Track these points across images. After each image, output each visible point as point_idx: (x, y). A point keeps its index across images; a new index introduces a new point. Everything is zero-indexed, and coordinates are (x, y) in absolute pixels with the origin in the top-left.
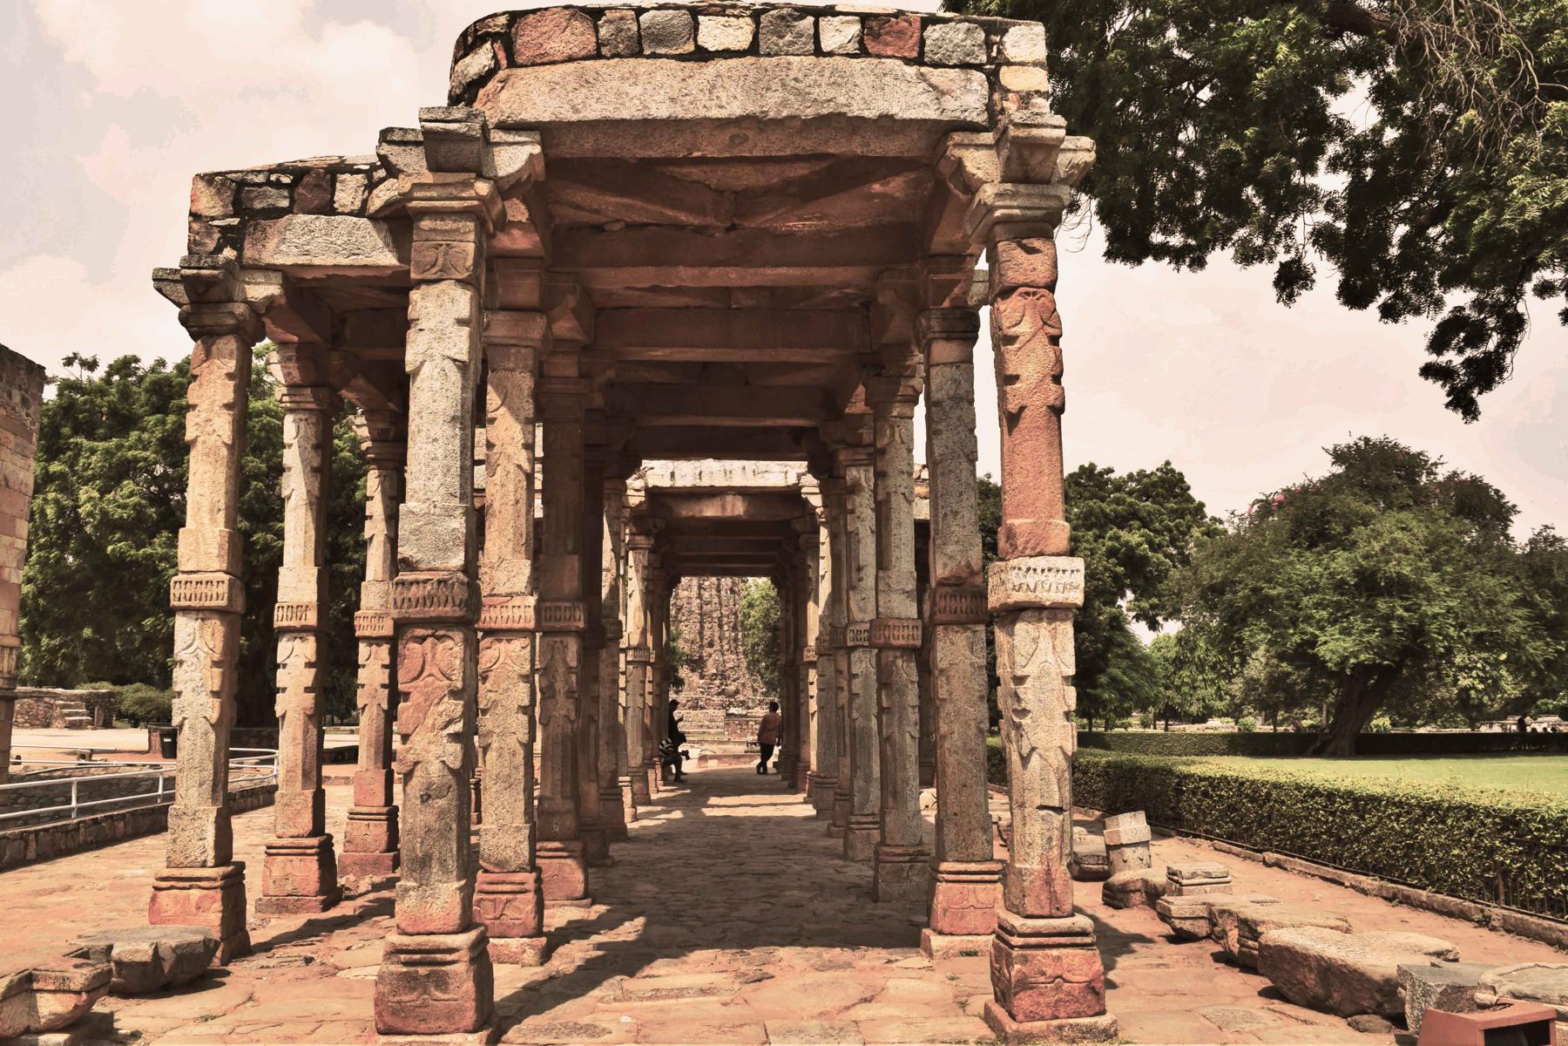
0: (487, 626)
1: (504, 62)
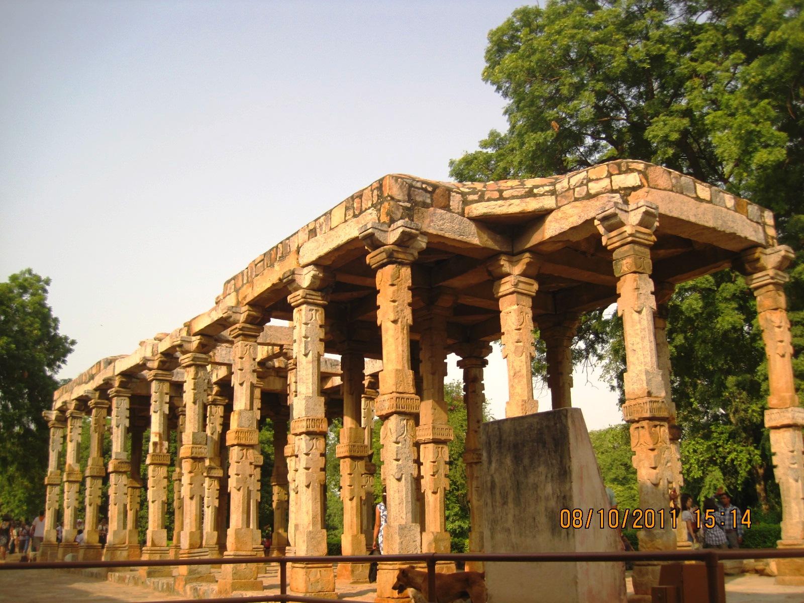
1: (646, 184)
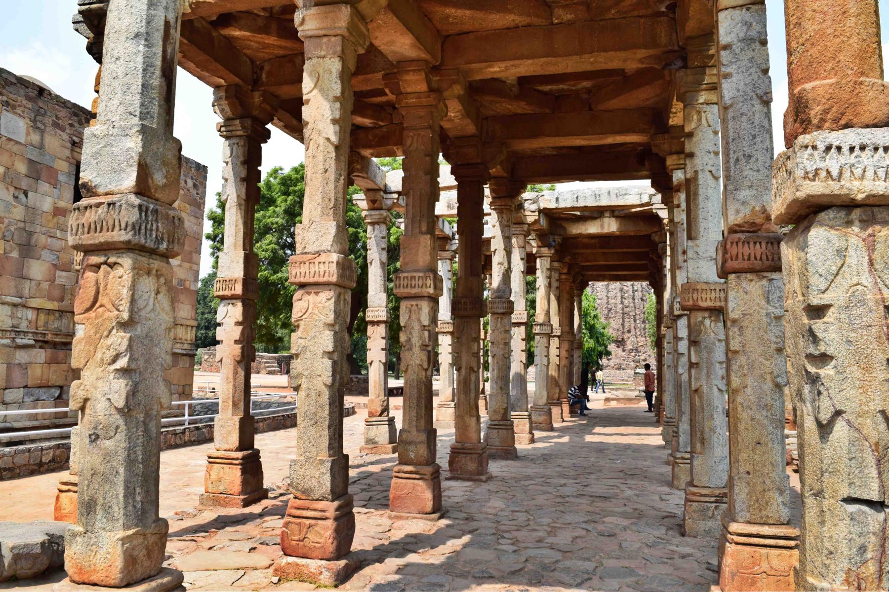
0: (298, 280)
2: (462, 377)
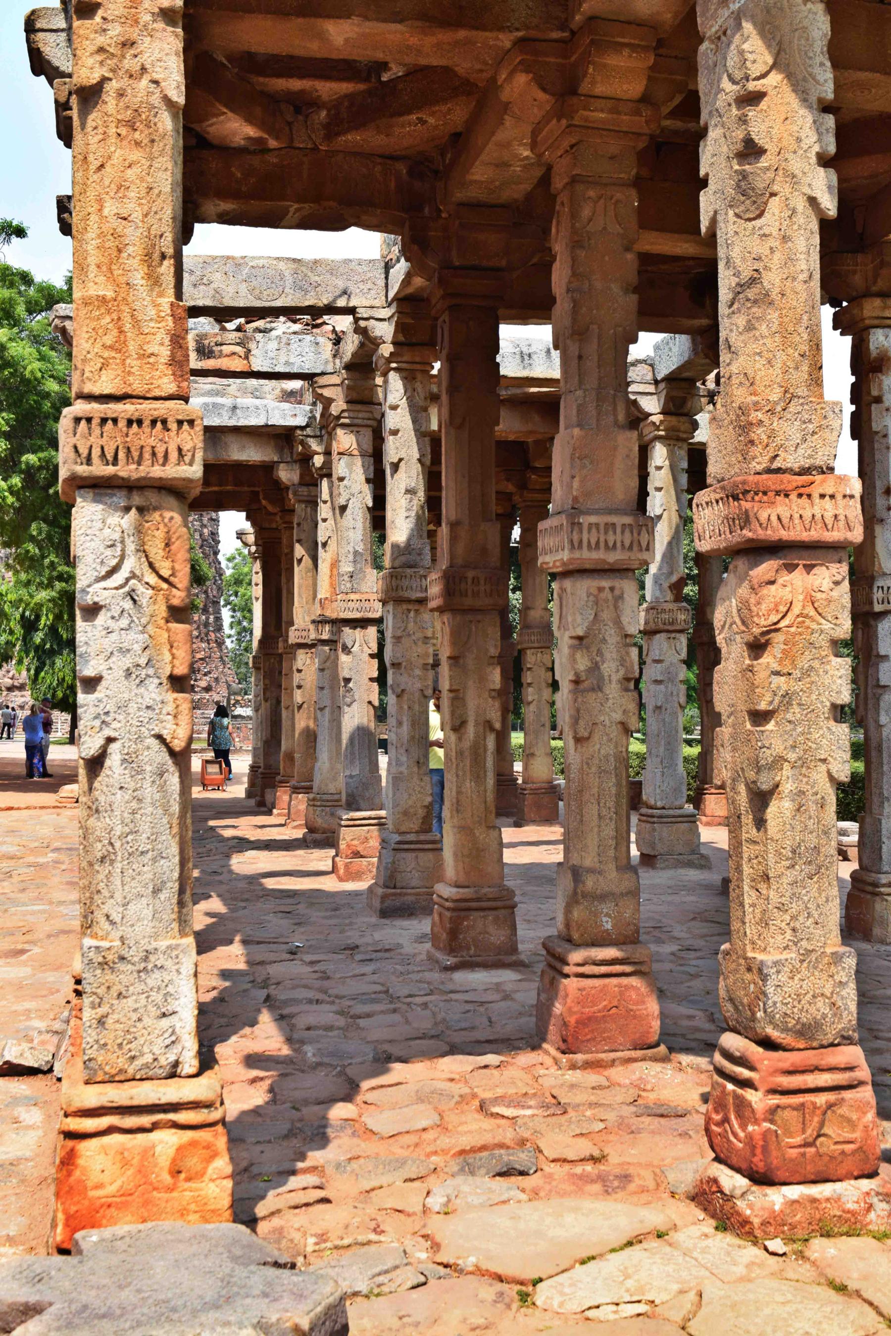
2: (467, 744)
